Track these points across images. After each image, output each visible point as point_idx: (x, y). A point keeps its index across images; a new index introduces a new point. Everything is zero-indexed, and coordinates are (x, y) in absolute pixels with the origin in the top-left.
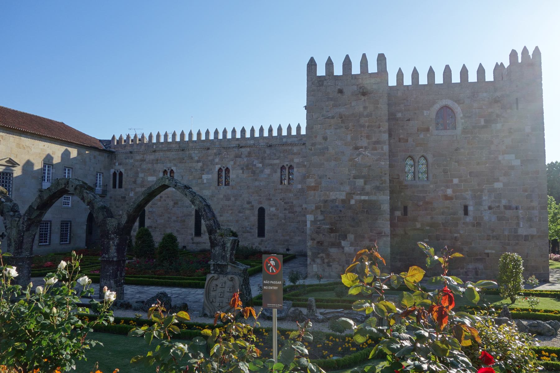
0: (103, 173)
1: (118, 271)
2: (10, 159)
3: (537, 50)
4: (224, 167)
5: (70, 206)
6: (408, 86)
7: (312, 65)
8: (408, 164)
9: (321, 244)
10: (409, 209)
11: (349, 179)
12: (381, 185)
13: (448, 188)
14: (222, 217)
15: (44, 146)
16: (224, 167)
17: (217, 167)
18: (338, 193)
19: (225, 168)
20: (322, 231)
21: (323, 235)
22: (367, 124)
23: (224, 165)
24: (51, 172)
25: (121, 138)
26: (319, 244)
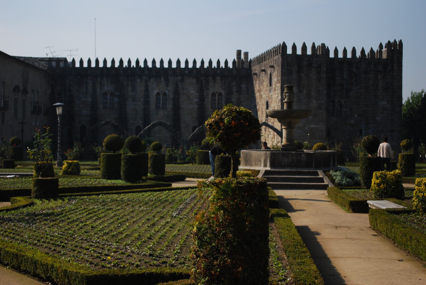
3: (401, 42)
7: (284, 46)
16: (161, 92)
17: (156, 92)
19: (163, 92)
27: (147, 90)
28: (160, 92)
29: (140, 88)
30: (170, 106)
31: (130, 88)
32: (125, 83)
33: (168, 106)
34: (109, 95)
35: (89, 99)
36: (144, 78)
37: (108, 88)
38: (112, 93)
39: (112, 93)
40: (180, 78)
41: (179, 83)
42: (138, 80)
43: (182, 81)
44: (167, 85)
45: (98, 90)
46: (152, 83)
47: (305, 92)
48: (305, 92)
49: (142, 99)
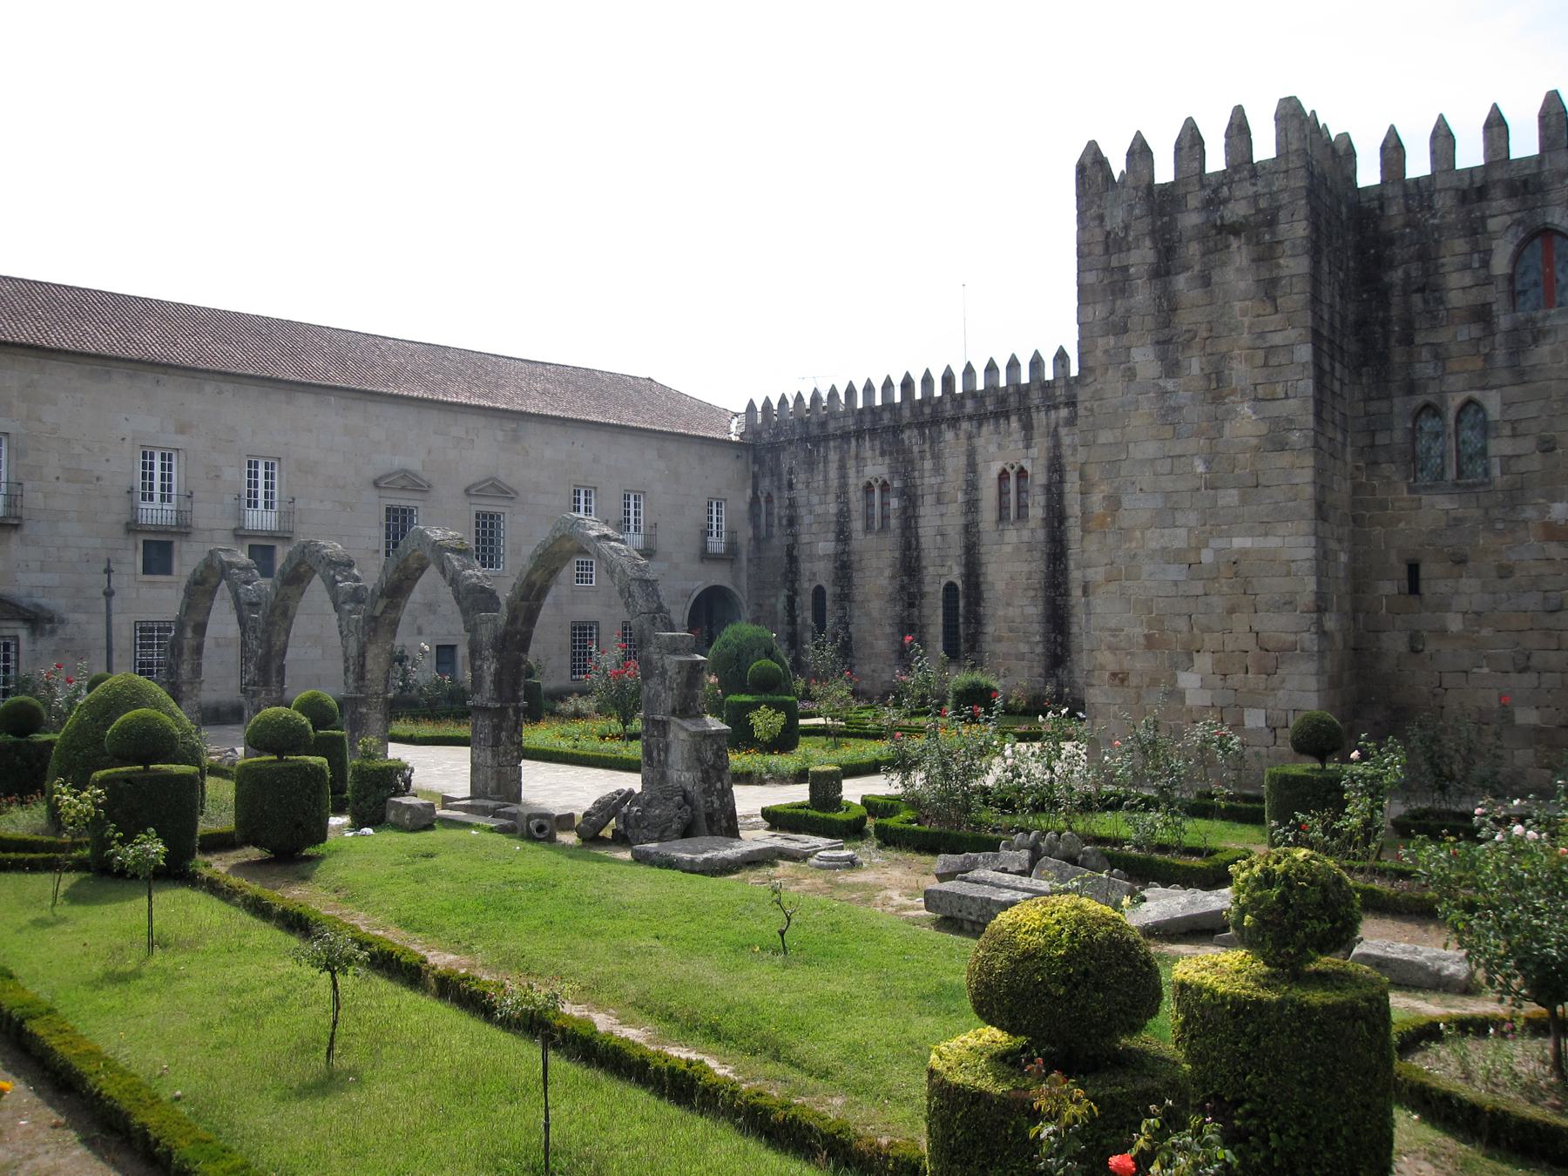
0: (725, 500)
1: (502, 729)
2: (494, 479)
4: (1013, 468)
5: (594, 584)
6: (1417, 181)
7: (1091, 166)
8: (1426, 429)
9: (1122, 680)
10: (1424, 572)
11: (1198, 489)
12: (1291, 504)
13: (1555, 501)
14: (1011, 609)
15: (573, 443)
16: (1013, 468)
17: (996, 468)
18: (1166, 531)
20: (1123, 644)
21: (1128, 654)
22: (1247, 321)
23: (1011, 462)
24: (593, 506)
25: (767, 402)
26: (1117, 682)
27: (972, 466)
28: (1008, 469)
29: (955, 463)
30: (1037, 511)
31: (928, 464)
32: (916, 449)
33: (1031, 512)
34: (877, 492)
35: (833, 508)
36: (965, 425)
37: (876, 468)
38: (885, 483)
39: (885, 483)
40: (1064, 412)
41: (1063, 431)
42: (949, 435)
43: (1071, 421)
44: (1028, 443)
45: (852, 480)
46: (987, 440)
47: (1195, 365)
48: (1195, 365)
49: (960, 497)
